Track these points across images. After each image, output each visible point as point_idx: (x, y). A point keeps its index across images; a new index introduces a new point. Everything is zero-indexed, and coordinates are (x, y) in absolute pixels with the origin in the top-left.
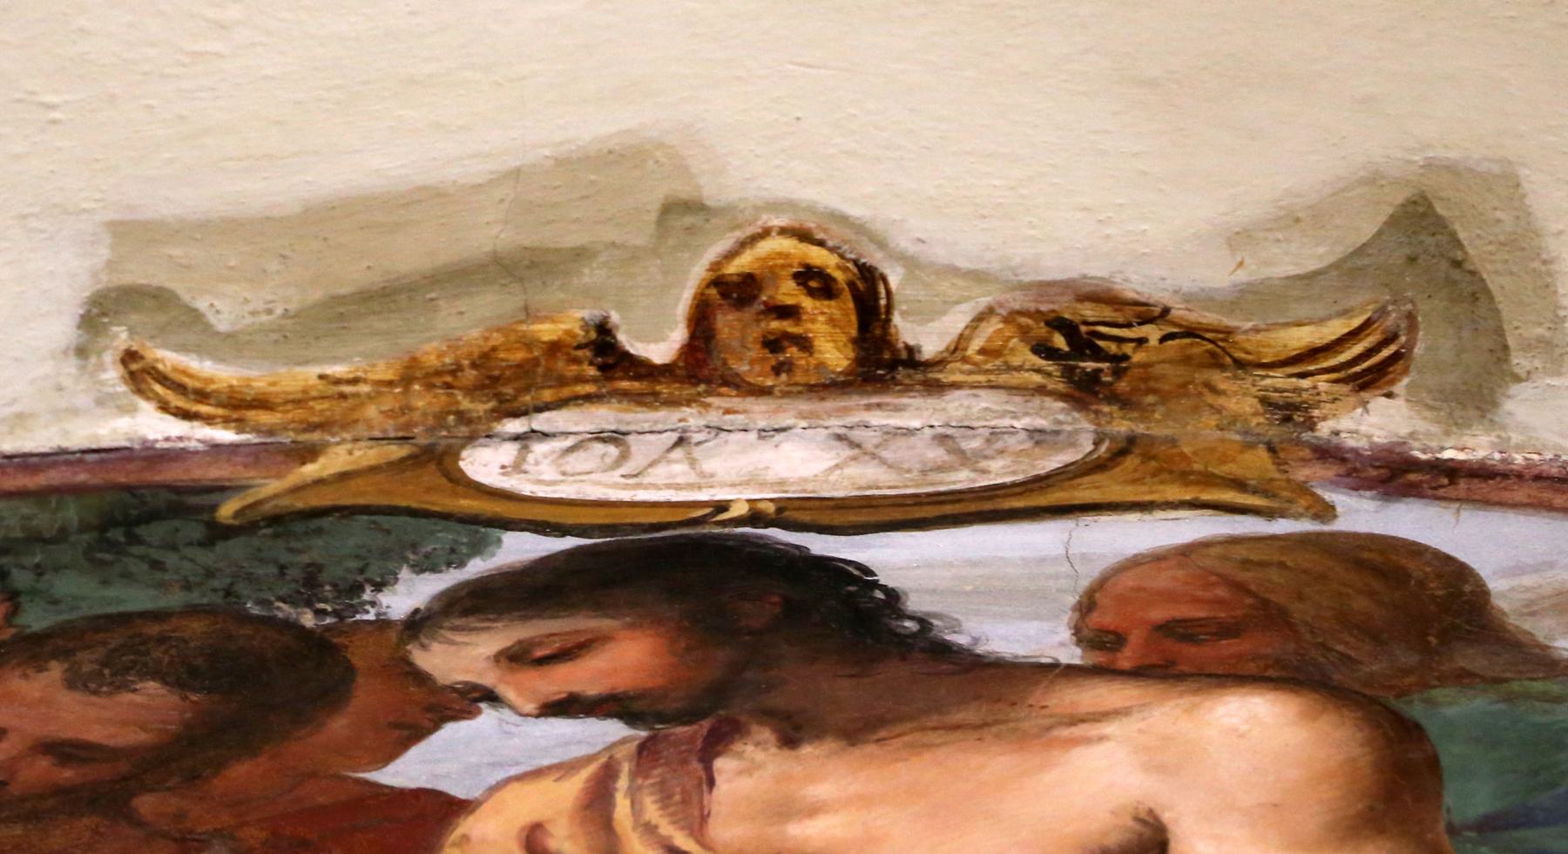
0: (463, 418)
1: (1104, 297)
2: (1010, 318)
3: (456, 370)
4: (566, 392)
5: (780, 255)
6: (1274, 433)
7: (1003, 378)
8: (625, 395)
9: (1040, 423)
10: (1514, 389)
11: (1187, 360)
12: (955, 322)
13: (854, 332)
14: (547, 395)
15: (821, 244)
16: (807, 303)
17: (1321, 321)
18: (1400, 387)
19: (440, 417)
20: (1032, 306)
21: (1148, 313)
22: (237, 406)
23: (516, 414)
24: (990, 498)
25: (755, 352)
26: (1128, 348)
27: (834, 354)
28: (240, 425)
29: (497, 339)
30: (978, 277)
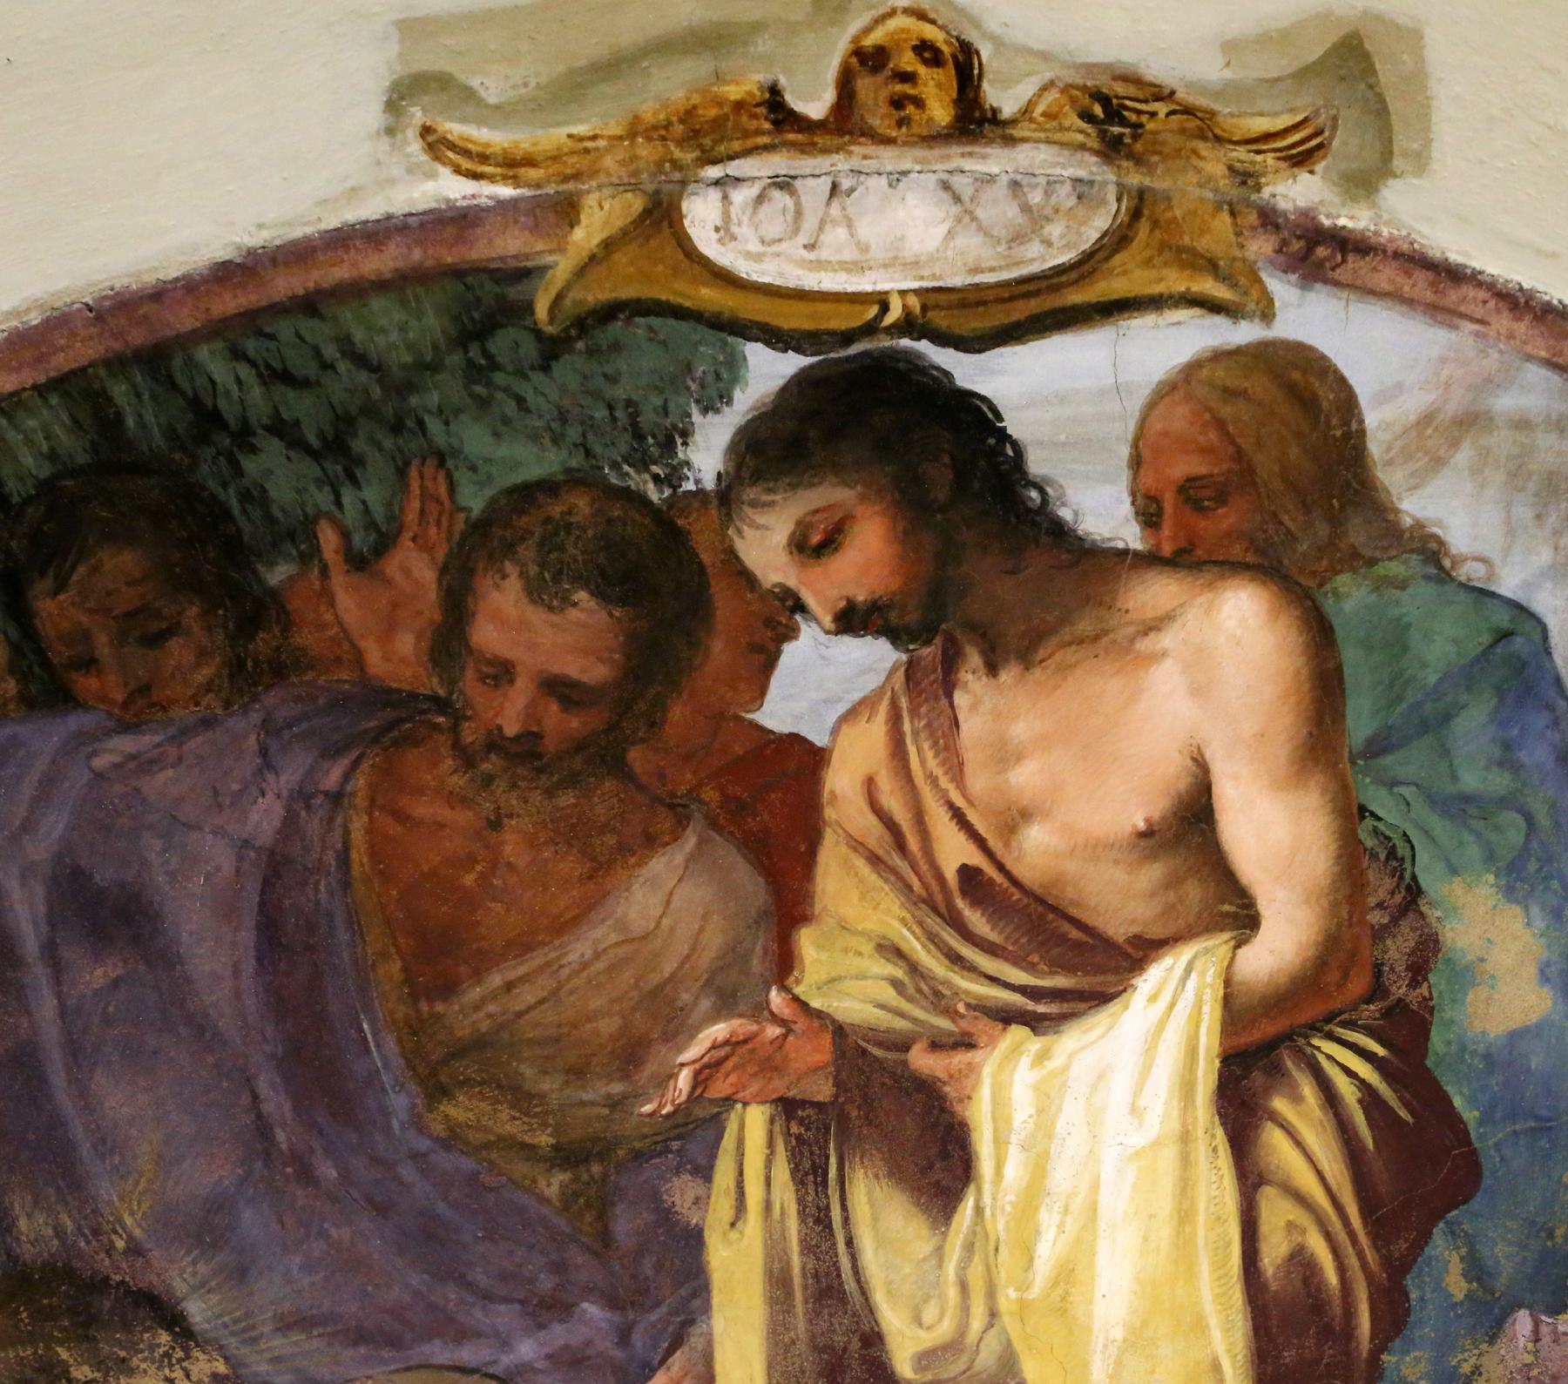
1: (1131, 78)
2: (1066, 89)
3: (668, 125)
4: (750, 143)
5: (903, 30)
6: (1235, 193)
7: (1058, 136)
8: (792, 145)
9: (1081, 173)
10: (1391, 182)
11: (1182, 131)
12: (1026, 90)
13: (954, 95)
14: (736, 146)
15: (933, 22)
16: (922, 70)
17: (1275, 114)
18: (1319, 168)
19: (659, 164)
20: (1080, 81)
21: (1160, 94)
22: (512, 164)
25: (884, 109)
26: (1144, 118)
27: (940, 112)
28: (516, 181)
29: (696, 99)
30: (1045, 56)
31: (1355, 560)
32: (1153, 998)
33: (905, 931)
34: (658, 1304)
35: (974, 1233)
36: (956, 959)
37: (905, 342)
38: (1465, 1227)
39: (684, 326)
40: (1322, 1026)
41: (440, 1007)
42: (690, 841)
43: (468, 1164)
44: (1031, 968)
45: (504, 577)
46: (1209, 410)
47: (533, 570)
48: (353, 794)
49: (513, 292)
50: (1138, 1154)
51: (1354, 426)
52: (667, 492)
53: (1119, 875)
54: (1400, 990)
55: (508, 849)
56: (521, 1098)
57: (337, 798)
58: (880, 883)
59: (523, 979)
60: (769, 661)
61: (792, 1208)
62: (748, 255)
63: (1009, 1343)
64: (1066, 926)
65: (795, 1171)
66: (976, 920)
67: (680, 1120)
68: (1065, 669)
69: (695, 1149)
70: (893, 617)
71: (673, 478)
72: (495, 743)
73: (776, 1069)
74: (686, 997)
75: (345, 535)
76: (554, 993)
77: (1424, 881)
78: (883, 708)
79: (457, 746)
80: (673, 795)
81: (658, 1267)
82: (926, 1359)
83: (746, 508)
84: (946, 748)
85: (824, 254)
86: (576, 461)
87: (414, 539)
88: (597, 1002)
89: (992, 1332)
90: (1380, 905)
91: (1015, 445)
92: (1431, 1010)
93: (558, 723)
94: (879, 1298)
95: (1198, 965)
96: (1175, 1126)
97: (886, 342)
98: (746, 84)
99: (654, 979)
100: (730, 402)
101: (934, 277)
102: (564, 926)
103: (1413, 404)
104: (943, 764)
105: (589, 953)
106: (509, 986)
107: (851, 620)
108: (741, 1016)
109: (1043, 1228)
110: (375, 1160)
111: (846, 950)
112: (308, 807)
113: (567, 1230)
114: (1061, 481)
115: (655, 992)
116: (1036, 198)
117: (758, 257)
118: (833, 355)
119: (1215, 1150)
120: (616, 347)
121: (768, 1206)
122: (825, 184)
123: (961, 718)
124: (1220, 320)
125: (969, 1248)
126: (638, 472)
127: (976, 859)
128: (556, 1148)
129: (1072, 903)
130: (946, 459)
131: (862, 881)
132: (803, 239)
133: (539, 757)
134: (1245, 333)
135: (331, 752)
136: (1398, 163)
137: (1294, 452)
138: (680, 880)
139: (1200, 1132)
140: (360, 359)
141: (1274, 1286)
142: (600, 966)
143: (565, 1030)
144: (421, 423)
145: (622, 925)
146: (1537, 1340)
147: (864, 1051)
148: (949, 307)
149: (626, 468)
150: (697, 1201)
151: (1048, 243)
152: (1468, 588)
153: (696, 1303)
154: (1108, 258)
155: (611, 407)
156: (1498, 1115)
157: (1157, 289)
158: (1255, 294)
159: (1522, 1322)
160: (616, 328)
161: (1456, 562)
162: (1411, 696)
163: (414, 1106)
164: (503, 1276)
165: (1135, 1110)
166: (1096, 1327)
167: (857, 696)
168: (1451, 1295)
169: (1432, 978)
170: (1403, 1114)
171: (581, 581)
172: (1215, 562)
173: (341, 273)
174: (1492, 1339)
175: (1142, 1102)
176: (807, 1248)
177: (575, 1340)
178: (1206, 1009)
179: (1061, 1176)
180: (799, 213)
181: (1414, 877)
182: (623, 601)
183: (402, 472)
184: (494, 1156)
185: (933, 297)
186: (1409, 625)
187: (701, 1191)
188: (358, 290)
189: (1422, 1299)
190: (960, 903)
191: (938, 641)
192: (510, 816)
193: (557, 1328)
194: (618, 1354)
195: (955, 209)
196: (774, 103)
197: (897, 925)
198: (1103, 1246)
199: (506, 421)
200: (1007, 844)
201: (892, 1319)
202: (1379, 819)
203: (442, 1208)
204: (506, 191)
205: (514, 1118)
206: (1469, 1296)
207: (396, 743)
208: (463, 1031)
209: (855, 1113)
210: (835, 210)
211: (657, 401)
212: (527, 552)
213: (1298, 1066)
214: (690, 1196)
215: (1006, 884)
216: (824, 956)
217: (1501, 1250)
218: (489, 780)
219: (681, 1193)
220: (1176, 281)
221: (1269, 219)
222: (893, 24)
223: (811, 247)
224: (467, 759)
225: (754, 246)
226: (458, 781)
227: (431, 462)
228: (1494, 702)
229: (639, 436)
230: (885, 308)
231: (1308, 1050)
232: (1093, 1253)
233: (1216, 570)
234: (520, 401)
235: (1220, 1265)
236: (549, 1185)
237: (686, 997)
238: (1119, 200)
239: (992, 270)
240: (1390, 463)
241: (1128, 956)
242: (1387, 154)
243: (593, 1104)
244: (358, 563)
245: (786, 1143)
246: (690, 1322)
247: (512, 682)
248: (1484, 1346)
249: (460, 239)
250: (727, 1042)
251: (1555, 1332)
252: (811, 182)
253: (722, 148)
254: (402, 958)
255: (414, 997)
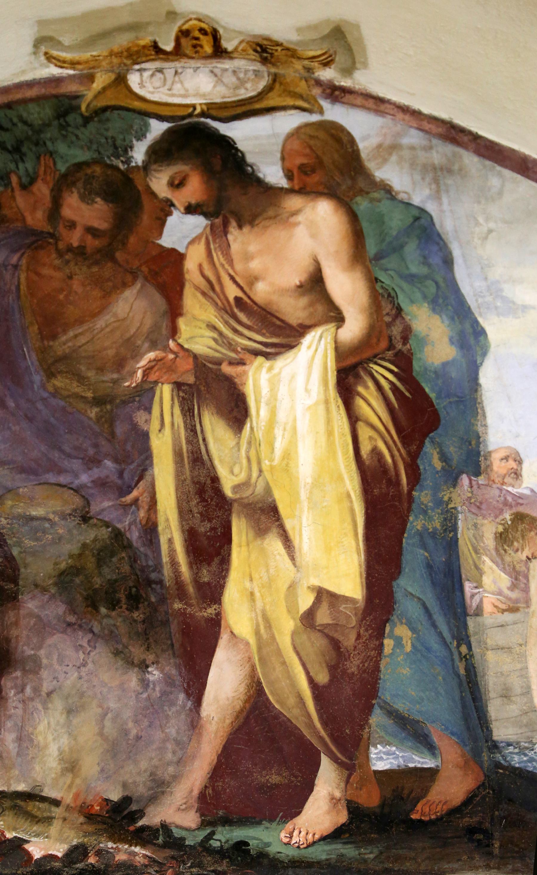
0: (125, 65)
2: (248, 43)
3: (122, 53)
6: (306, 74)
11: (287, 55)
12: (235, 43)
16: (201, 37)
20: (252, 40)
22: (73, 64)
23: (138, 64)
24: (250, 103)
26: (274, 52)
28: (74, 69)
29: (130, 45)
31: (362, 192)
32: (309, 347)
33: (217, 320)
34: (133, 462)
35: (251, 438)
36: (235, 331)
37: (202, 120)
38: (437, 440)
39: (130, 114)
40: (373, 359)
41: (51, 343)
42: (138, 285)
43: (62, 403)
44: (263, 335)
45: (72, 193)
46: (306, 142)
47: (82, 191)
48: (21, 266)
49: (74, 103)
50: (309, 408)
51: (355, 148)
52: (126, 166)
53: (292, 301)
54: (399, 346)
55: (75, 287)
56: (81, 379)
57: (16, 267)
58: (206, 302)
59: (80, 334)
60: (162, 223)
61: (182, 425)
62: (150, 92)
63: (268, 483)
64: (275, 320)
65: (182, 410)
66: (242, 316)
67: (139, 389)
68: (266, 228)
69: (145, 400)
70: (205, 209)
71: (128, 161)
72: (70, 249)
73: (173, 371)
74: (139, 342)
75: (20, 178)
76: (93, 338)
77: (403, 305)
78: (203, 240)
79: (57, 249)
80: (132, 269)
81: (133, 447)
82: (236, 488)
83: (153, 172)
84: (226, 254)
85: (174, 92)
86: (95, 155)
87: (42, 180)
88: (107, 344)
89: (261, 478)
90: (388, 314)
91: (242, 152)
92: (412, 354)
93: (92, 243)
94: (216, 463)
95: (325, 335)
96: (322, 397)
97: (196, 119)
98: (146, 40)
99: (128, 335)
100: (146, 137)
101: (210, 99)
102: (95, 315)
103: (374, 141)
104: (225, 260)
105: (104, 325)
106: (76, 336)
107: (190, 210)
108: (159, 350)
109: (277, 436)
110: (29, 400)
111: (196, 327)
112: (6, 270)
113: (99, 431)
114: (258, 164)
115: (129, 340)
116: (242, 75)
117: (152, 93)
118: (179, 123)
119: (338, 407)
120: (108, 120)
121: (173, 424)
122: (173, 71)
123: (231, 243)
124: (306, 114)
125: (249, 443)
126: (116, 159)
127: (240, 294)
128: (94, 398)
129: (277, 311)
130: (219, 157)
131: (200, 301)
132: (167, 87)
133: (85, 254)
134: (315, 118)
135: (14, 251)
136: (358, 65)
137: (336, 156)
138: (135, 299)
139: (332, 400)
140: (25, 123)
141: (367, 463)
142: (108, 330)
143: (96, 353)
144: (45, 143)
145: (115, 315)
146: (471, 487)
147: (205, 365)
148: (216, 109)
149: (112, 158)
150: (146, 421)
151: (246, 89)
152: (402, 202)
153: (148, 462)
154: (266, 94)
155: (106, 139)
156: (443, 396)
157: (284, 104)
158: (316, 106)
159: (465, 480)
160: (108, 114)
161: (397, 193)
162: (388, 239)
163: (42, 380)
164: (76, 448)
165: (307, 390)
166: (300, 477)
167: (194, 235)
168: (435, 468)
169: (410, 341)
170: (407, 394)
171: (98, 194)
172: (314, 192)
173: (19, 96)
174: (454, 486)
175: (309, 387)
176: (188, 442)
177: (103, 475)
178: (329, 352)
179: (282, 416)
180: (165, 80)
181: (398, 304)
182: (112, 202)
183: (38, 158)
184: (71, 400)
185: (211, 106)
186: (383, 215)
187: (147, 417)
188: (25, 101)
189: (425, 469)
190: (236, 310)
191: (221, 217)
192: (75, 275)
193: (96, 470)
194: (119, 482)
195: (215, 79)
196: (155, 46)
197: (213, 317)
198: (300, 445)
199: (72, 142)
200: (251, 289)
201: (222, 472)
202: (383, 282)
203: (52, 420)
204: (71, 72)
205: (78, 386)
206: (443, 468)
207: (36, 248)
208: (59, 353)
209: (203, 388)
210: (177, 79)
211: (121, 137)
212: (80, 185)
213: (365, 374)
214: (144, 418)
215: (252, 304)
216: (188, 329)
217: (452, 449)
218: (68, 262)
219: (140, 417)
220: (290, 102)
221: (318, 83)
222: (191, 23)
223: (170, 90)
224: (60, 254)
225: (151, 89)
226: (57, 262)
227: (48, 156)
228: (417, 242)
229: (116, 148)
230: (195, 109)
231: (368, 368)
232: (296, 446)
233: (314, 195)
234: (77, 136)
235: (346, 453)
236: (91, 413)
237: (139, 342)
238: (269, 76)
239: (229, 97)
240: (369, 160)
241: (297, 331)
242: (354, 63)
243: (107, 382)
244: (24, 187)
245: (178, 399)
246: (145, 470)
247: (75, 228)
248: (452, 489)
249: (57, 86)
250: (154, 360)
251: (478, 484)
252: (169, 70)
253: (139, 60)
254: (38, 324)
255: (42, 339)
